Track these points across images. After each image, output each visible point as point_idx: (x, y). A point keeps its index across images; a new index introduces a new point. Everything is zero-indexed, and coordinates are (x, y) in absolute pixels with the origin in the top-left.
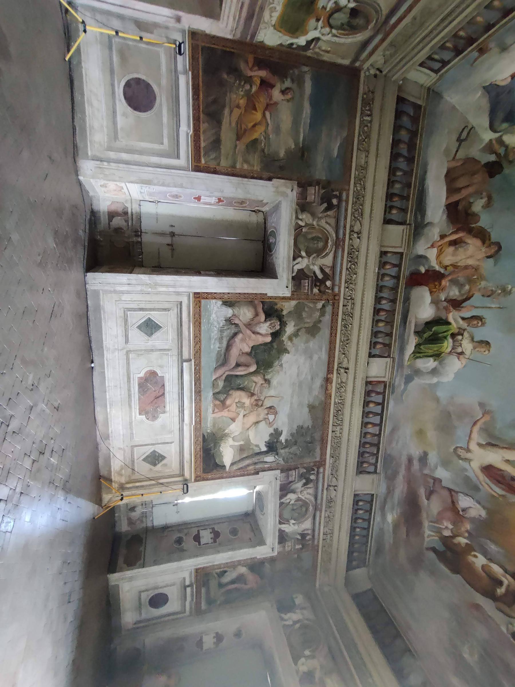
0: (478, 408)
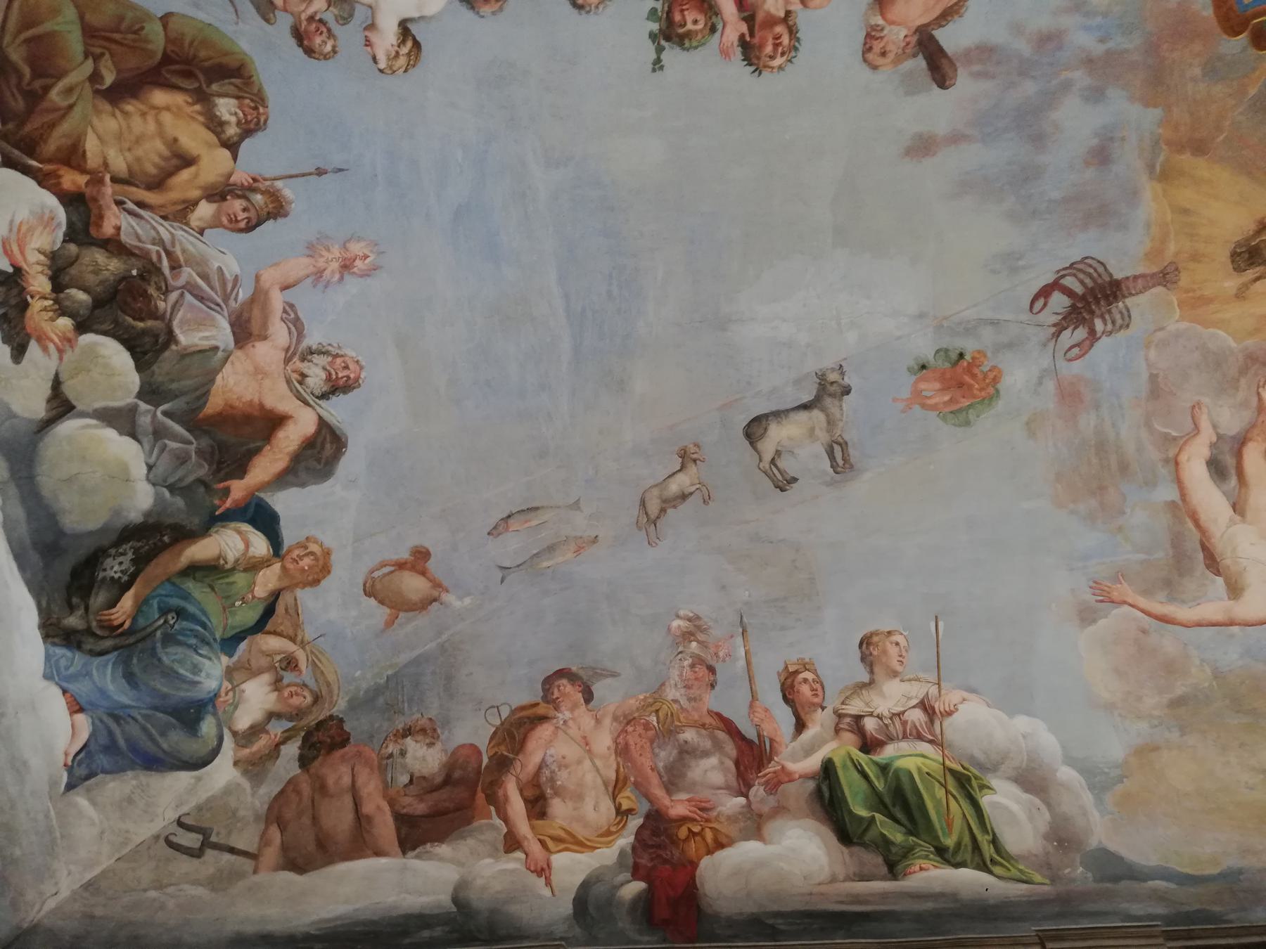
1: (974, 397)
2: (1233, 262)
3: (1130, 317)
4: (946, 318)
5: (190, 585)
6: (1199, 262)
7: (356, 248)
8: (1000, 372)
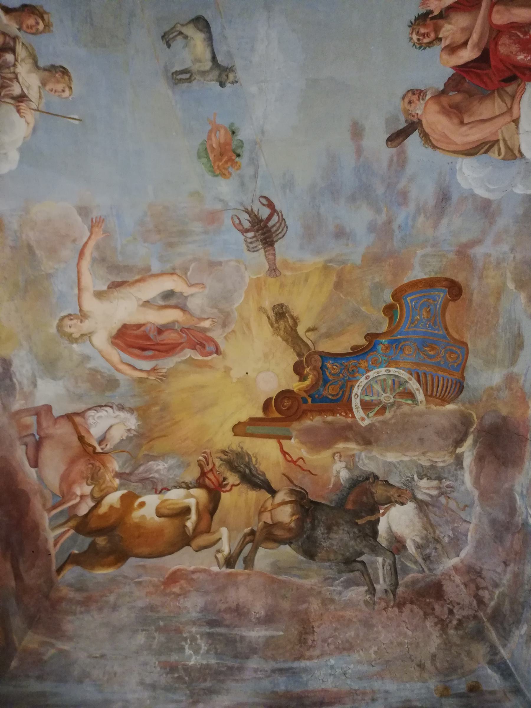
0: (79, 219)
1: (215, 162)
2: (279, 305)
3: (253, 251)
4: (260, 147)
8: (228, 178)
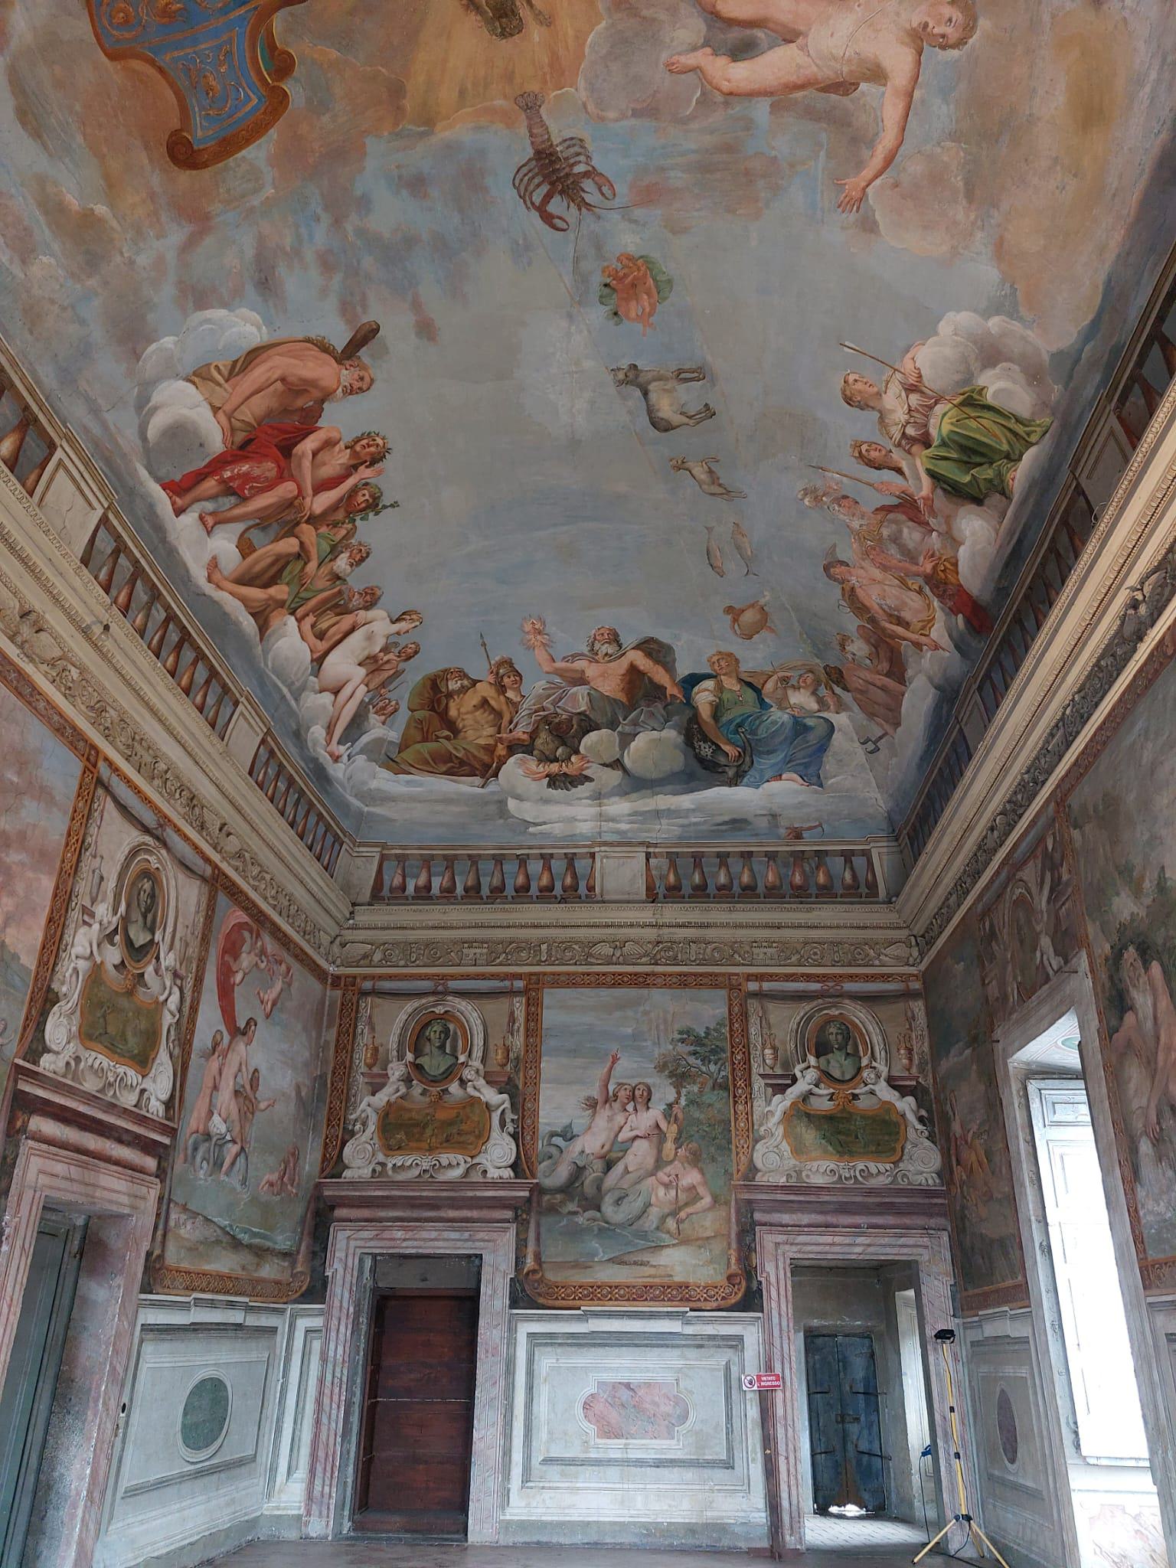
0: (878, 217)
2: (512, 35)
3: (572, 139)
5: (724, 719)
6: (513, 72)
7: (528, 627)
